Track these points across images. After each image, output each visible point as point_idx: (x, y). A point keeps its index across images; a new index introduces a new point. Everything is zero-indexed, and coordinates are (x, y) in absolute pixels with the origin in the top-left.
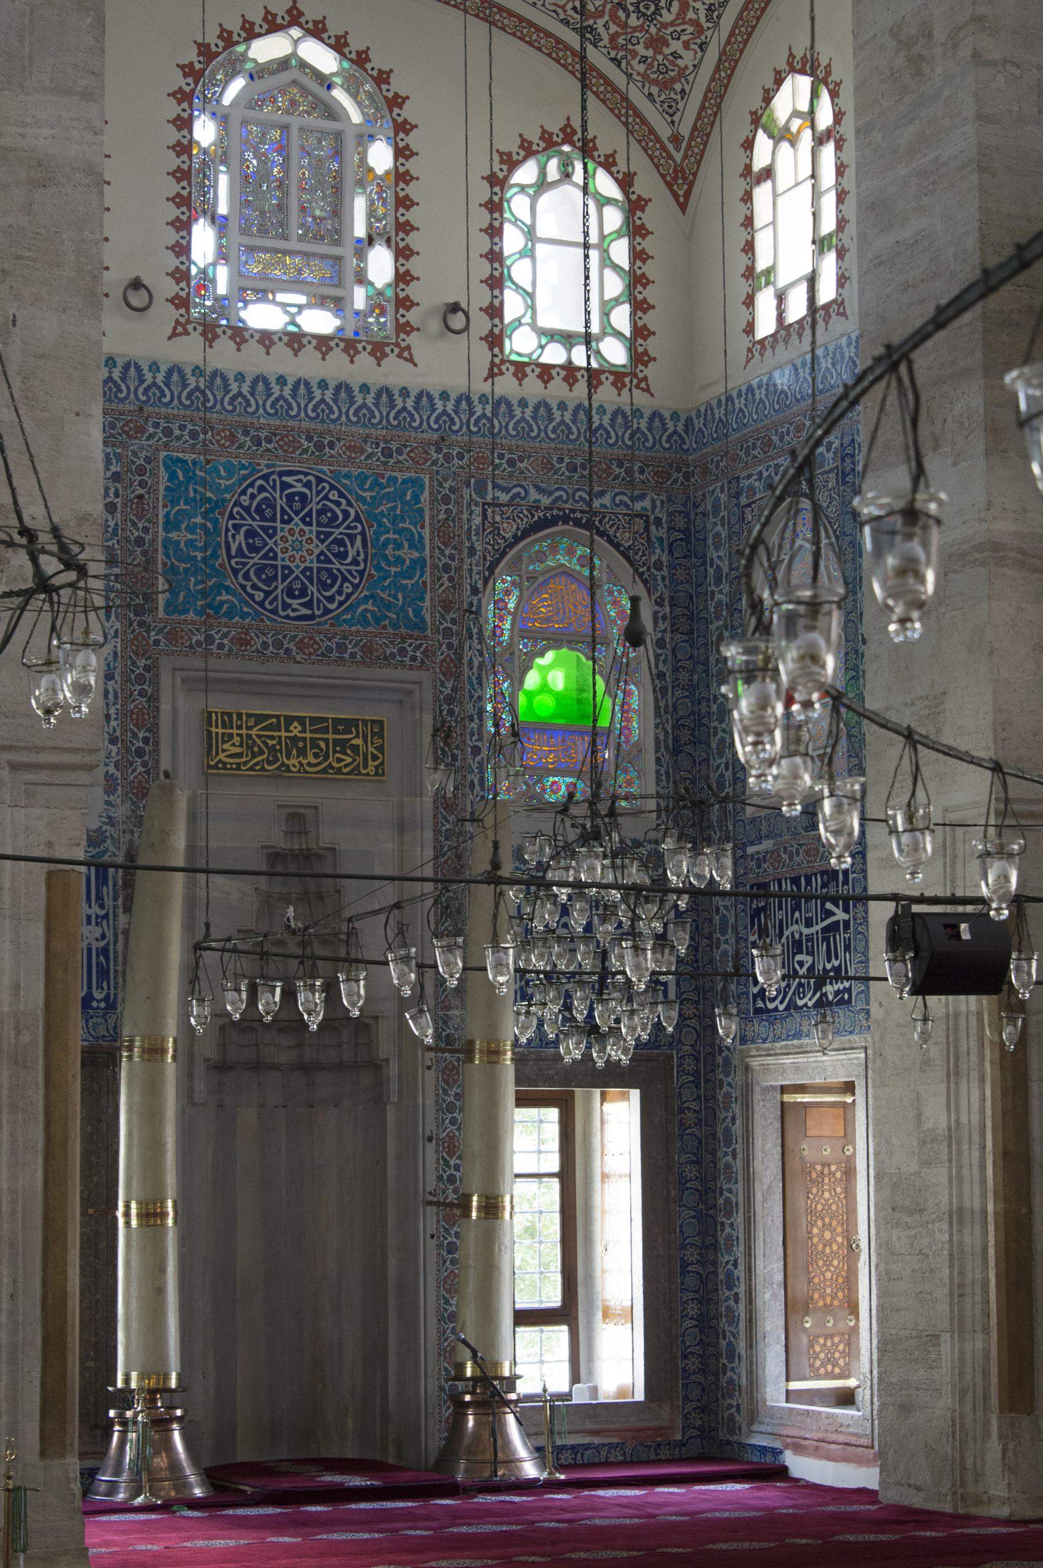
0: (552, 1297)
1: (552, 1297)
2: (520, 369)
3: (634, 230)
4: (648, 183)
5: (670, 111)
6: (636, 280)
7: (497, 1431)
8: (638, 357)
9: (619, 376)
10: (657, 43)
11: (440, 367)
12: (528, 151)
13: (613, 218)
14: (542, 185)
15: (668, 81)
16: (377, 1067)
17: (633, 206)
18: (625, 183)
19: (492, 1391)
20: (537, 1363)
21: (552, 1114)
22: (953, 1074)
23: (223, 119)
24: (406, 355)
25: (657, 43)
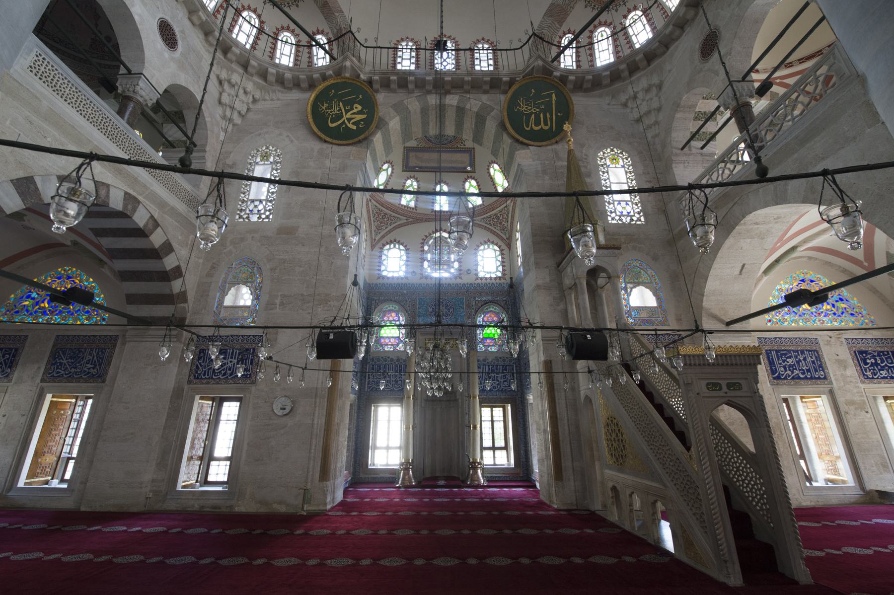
0: (503, 445)
1: (503, 445)
2: (481, 279)
3: (502, 254)
4: (504, 247)
5: (505, 234)
6: (503, 262)
7: (476, 473)
8: (504, 274)
9: (500, 278)
10: (500, 223)
11: (467, 280)
12: (482, 244)
13: (498, 253)
14: (485, 249)
15: (503, 229)
16: (456, 400)
17: (501, 251)
18: (499, 247)
19: (474, 465)
20: (488, 459)
21: (501, 409)
22: (542, 398)
23: (429, 246)
24: (461, 278)
25: (500, 223)
